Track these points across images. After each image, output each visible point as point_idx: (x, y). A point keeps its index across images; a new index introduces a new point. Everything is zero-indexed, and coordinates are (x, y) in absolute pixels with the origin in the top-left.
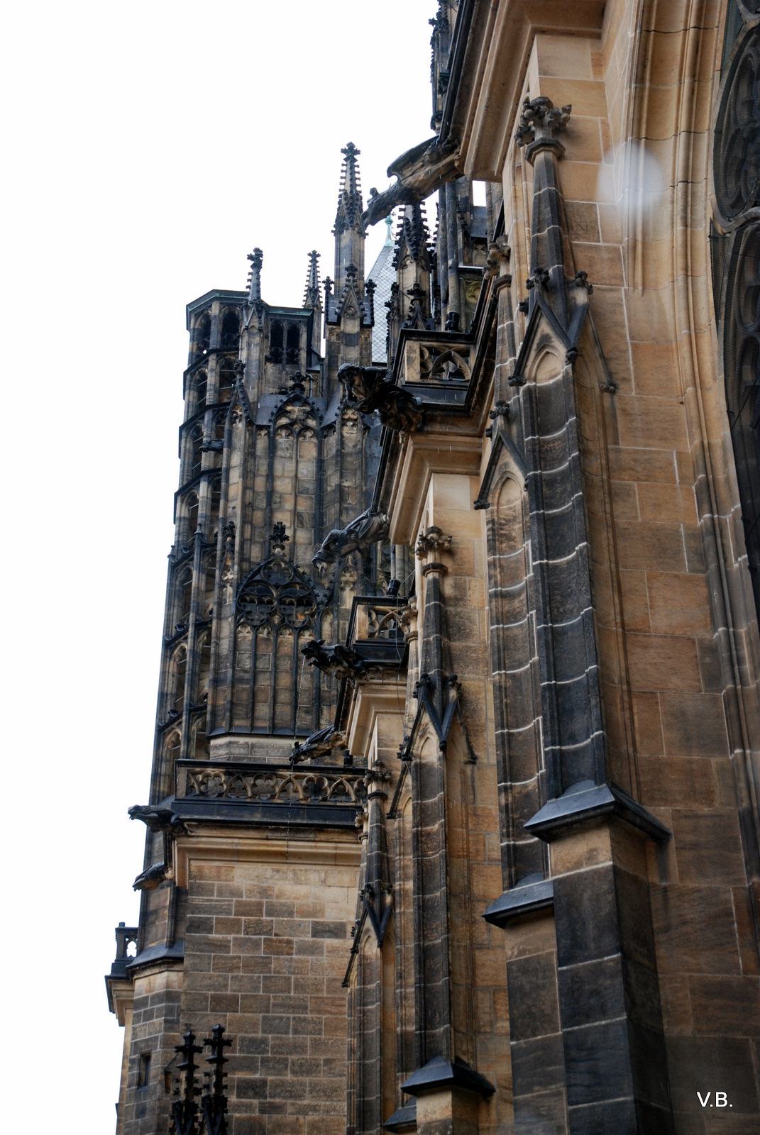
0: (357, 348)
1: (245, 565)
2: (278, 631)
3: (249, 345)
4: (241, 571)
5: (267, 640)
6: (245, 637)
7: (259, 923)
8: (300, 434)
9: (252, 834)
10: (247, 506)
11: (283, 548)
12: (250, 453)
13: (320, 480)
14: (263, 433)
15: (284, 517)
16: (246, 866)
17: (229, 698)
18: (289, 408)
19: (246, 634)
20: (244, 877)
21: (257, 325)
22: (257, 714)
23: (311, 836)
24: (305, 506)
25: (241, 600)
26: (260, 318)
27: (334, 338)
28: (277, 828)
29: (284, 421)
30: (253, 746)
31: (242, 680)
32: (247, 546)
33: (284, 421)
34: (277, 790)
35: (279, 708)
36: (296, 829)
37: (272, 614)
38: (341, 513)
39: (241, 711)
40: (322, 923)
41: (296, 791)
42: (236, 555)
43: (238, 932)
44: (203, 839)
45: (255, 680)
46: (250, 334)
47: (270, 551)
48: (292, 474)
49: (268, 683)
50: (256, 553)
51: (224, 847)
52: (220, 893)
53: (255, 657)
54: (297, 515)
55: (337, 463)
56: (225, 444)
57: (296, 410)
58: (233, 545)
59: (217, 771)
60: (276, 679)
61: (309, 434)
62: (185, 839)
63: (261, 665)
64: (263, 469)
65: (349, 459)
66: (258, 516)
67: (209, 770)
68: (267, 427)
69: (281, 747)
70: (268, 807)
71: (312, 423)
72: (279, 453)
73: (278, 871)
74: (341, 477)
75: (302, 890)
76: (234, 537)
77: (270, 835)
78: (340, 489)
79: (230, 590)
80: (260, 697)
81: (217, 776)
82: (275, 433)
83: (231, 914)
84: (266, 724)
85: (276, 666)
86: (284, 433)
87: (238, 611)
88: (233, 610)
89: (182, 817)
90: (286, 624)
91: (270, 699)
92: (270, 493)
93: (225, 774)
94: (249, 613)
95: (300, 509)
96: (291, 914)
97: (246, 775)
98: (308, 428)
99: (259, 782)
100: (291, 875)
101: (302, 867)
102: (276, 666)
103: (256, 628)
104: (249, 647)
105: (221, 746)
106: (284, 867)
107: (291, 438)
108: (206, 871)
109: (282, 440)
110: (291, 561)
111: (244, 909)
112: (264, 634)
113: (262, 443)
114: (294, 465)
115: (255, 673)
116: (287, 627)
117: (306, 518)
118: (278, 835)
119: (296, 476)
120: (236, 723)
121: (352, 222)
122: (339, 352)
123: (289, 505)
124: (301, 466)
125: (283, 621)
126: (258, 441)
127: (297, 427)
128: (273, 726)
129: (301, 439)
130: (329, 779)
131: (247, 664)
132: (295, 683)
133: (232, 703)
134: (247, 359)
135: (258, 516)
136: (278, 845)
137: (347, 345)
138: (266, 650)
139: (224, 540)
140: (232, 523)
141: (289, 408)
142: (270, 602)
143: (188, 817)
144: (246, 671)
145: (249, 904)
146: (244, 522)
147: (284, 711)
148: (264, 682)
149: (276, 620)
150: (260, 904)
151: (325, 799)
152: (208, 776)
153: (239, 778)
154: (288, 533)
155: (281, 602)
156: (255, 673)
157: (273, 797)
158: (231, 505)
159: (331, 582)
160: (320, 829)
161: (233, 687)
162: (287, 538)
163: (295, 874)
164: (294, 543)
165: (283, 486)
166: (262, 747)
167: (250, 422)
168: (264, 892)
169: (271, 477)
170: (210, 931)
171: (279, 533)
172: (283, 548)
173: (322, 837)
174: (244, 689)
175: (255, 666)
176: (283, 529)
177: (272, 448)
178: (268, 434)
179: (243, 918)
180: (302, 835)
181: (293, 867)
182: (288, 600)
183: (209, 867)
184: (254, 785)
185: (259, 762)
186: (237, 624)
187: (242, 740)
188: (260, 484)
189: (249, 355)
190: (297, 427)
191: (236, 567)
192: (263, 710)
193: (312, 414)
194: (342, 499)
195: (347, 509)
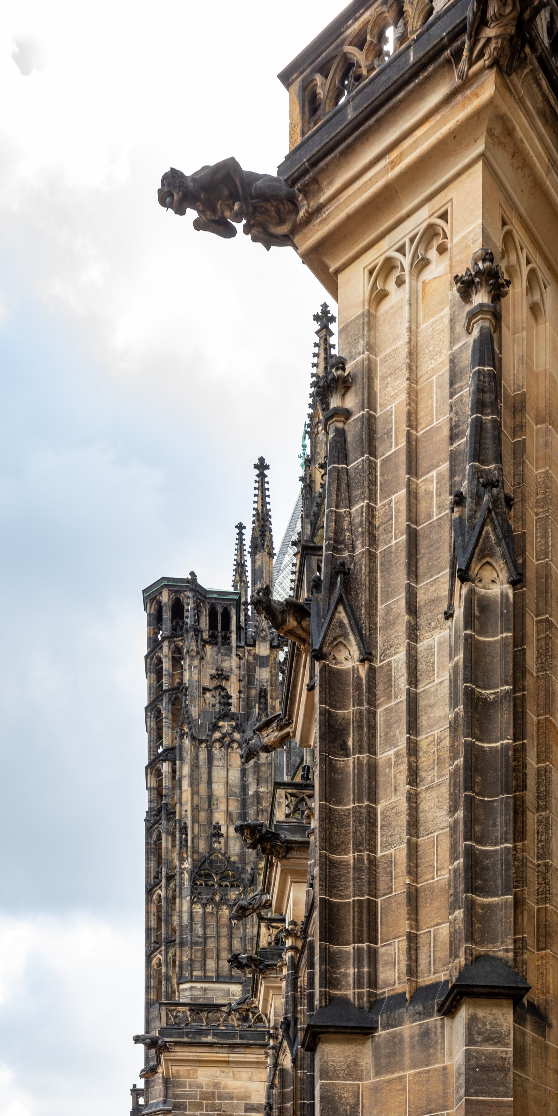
0: (268, 669)
1: (196, 856)
2: (218, 905)
3: (190, 666)
4: (193, 860)
5: (212, 913)
6: (197, 912)
7: (213, 1104)
8: (229, 746)
9: (206, 1049)
10: (195, 808)
11: (220, 843)
12: (195, 767)
13: (244, 787)
14: (203, 745)
15: (219, 817)
16: (205, 1069)
17: (189, 957)
18: (221, 723)
19: (198, 909)
20: (204, 1076)
21: (195, 648)
22: (207, 968)
23: (242, 1050)
24: (234, 807)
25: (194, 884)
26: (197, 641)
27: (251, 658)
28: (221, 1045)
29: (217, 735)
30: (205, 990)
31: (196, 943)
32: (196, 841)
33: (217, 735)
34: (221, 1020)
35: (221, 963)
36: (233, 1047)
37: (214, 894)
38: (258, 815)
39: (197, 965)
40: (250, 1104)
41: (233, 1020)
42: (189, 849)
43: (202, 1110)
44: (179, 1054)
45: (205, 943)
46: (192, 658)
47: (211, 845)
48: (225, 781)
49: (213, 945)
50: (202, 846)
51: (191, 1058)
52: (190, 1087)
53: (205, 927)
54: (229, 815)
55: (254, 772)
56: (178, 758)
57: (226, 726)
58: (187, 841)
59: (184, 1008)
60: (218, 942)
61: (235, 745)
62: (168, 1054)
63: (209, 932)
64: (204, 777)
65: (263, 769)
66: (203, 815)
67: (180, 1008)
68: (206, 741)
69: (223, 990)
70: (215, 1035)
71: (237, 736)
72: (216, 763)
73: (223, 1072)
74: (258, 784)
75: (238, 1084)
76: (187, 835)
77: (217, 1050)
78: (257, 794)
79: (186, 876)
80: (209, 955)
81: (184, 1012)
82: (212, 746)
83: (196, 1099)
84: (213, 974)
85: (218, 933)
86: (217, 745)
87: (192, 893)
88: (189, 892)
89: (166, 1039)
90: (224, 901)
91: (215, 957)
92: (210, 798)
93: (191, 1010)
94: (200, 894)
95: (231, 809)
96: (231, 1098)
97: (202, 1011)
98: (233, 741)
99: (210, 1014)
100: (231, 1074)
101: (237, 1069)
102: (218, 933)
103: (204, 906)
104: (200, 919)
105: (186, 989)
106: (226, 1070)
107: (223, 749)
108: (181, 1073)
109: (217, 752)
110: (226, 853)
111: (205, 1096)
112: (209, 909)
113: (203, 755)
114: (226, 773)
115: (205, 937)
116: (225, 904)
117: (235, 817)
118: (222, 1050)
119: (227, 782)
120: (195, 973)
121: (263, 545)
122: (255, 672)
123: (223, 807)
124: (230, 773)
125: (221, 899)
126: (200, 753)
127: (227, 740)
128: (218, 976)
129: (230, 750)
130: (252, 1013)
131: (200, 932)
132: (231, 945)
133: (191, 960)
134: (189, 680)
135: (203, 815)
136: (223, 1056)
137: (260, 666)
138: (211, 920)
139: (181, 837)
140: (185, 823)
141: (221, 723)
142: (213, 885)
143: (168, 1040)
144: (199, 937)
145: (207, 1092)
146: (193, 822)
147: (225, 965)
148: (211, 944)
149: (217, 898)
150: (213, 1093)
151: (250, 1027)
152: (179, 1012)
153: (198, 1013)
154: (223, 830)
155: (220, 886)
156: (205, 937)
157: (219, 1025)
158: (184, 808)
159: (252, 869)
160: (248, 1046)
161: (191, 949)
162: (222, 835)
163: (233, 1074)
164: (227, 837)
165: (219, 790)
166: (211, 990)
167: (194, 739)
168: (216, 1085)
169: (210, 783)
170: (185, 1109)
171: (216, 833)
172: (220, 843)
173: (248, 1050)
174: (199, 950)
175: (205, 933)
176: (219, 828)
177: (210, 758)
178: (207, 747)
179: (204, 1101)
180: (236, 1050)
181: (232, 1069)
182: (224, 884)
183: (183, 1069)
184: (207, 1017)
185: (210, 1002)
186: (192, 902)
187: (199, 985)
188: (203, 788)
189: (191, 676)
190: (227, 740)
191: (190, 859)
192: (211, 964)
193: (238, 728)
194: (259, 803)
195: (262, 810)
